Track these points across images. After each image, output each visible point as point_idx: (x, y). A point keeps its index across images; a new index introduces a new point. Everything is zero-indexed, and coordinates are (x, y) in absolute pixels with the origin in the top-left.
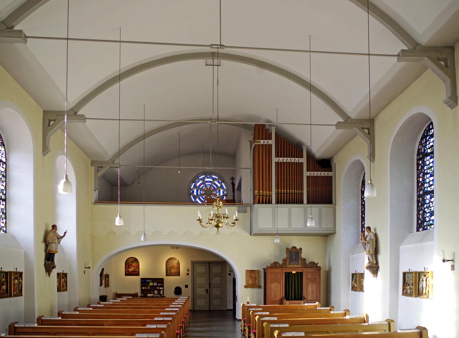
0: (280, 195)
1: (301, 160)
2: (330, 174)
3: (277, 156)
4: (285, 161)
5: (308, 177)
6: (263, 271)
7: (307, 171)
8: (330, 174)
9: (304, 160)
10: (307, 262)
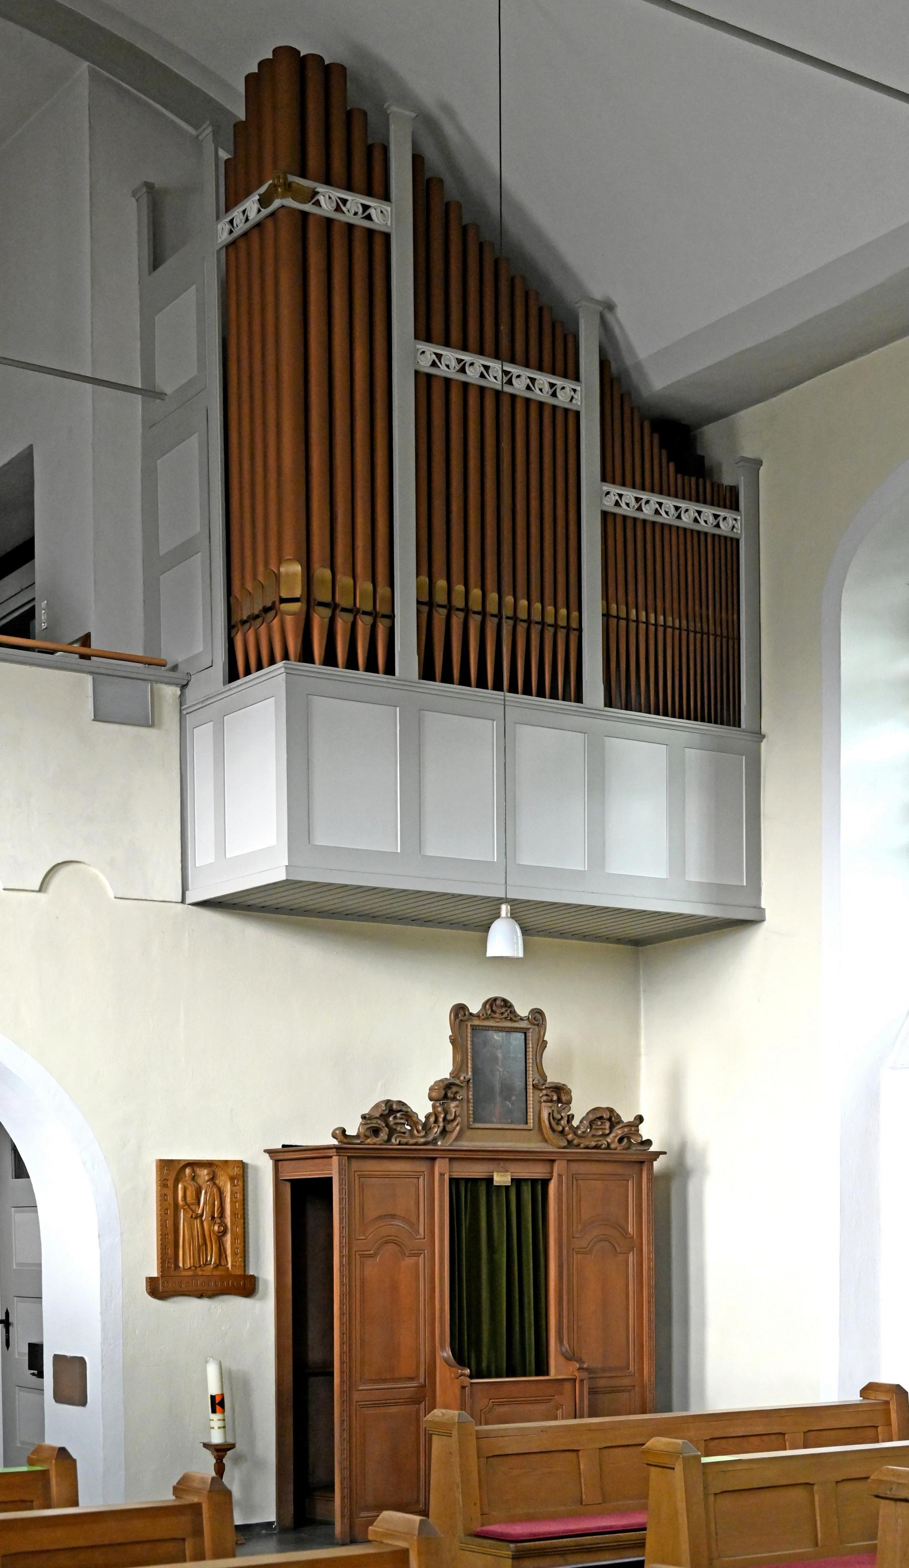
0: (440, 615)
2: (730, 523)
4: (472, 375)
6: (266, 1166)
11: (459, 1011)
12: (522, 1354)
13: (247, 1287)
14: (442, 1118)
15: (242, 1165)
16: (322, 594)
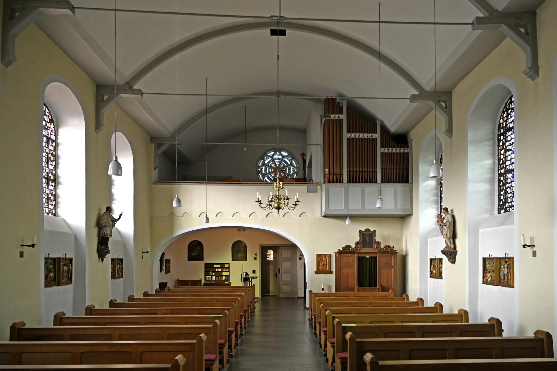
0: (351, 173)
1: (374, 136)
2: (406, 150)
3: (349, 131)
4: (357, 136)
5: (382, 153)
6: (334, 255)
7: (381, 147)
8: (406, 150)
9: (377, 136)
10: (382, 246)
11: (360, 231)
12: (372, 283)
13: (331, 273)
14: (357, 248)
15: (330, 255)
16: (332, 172)
